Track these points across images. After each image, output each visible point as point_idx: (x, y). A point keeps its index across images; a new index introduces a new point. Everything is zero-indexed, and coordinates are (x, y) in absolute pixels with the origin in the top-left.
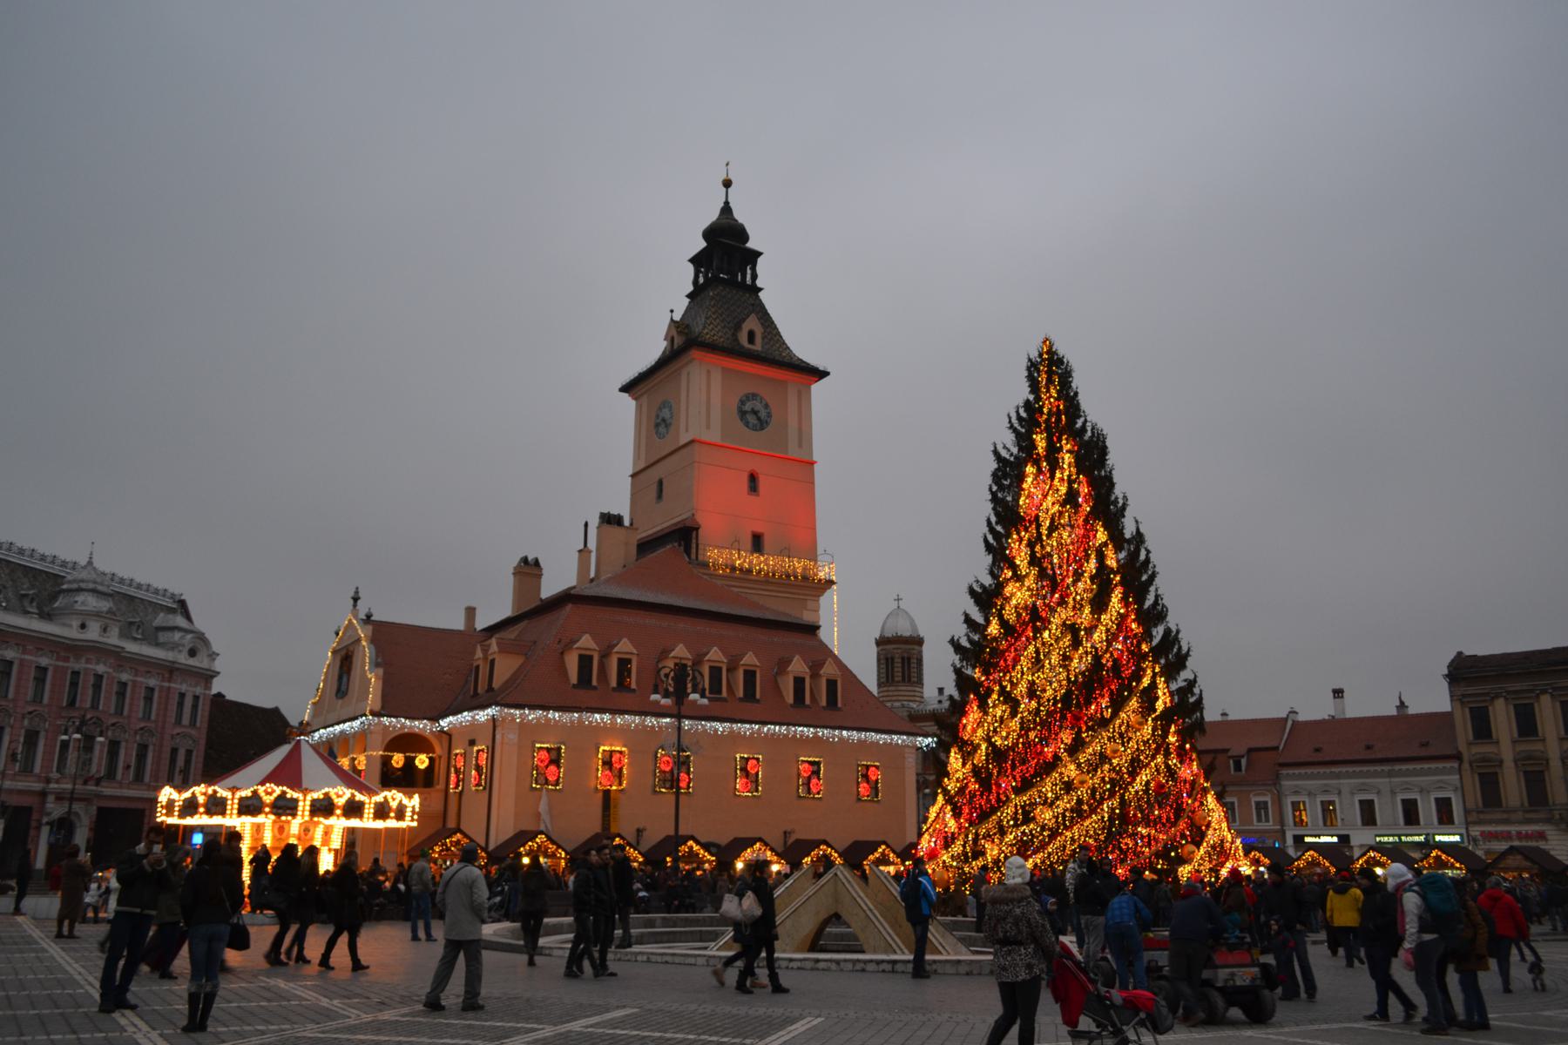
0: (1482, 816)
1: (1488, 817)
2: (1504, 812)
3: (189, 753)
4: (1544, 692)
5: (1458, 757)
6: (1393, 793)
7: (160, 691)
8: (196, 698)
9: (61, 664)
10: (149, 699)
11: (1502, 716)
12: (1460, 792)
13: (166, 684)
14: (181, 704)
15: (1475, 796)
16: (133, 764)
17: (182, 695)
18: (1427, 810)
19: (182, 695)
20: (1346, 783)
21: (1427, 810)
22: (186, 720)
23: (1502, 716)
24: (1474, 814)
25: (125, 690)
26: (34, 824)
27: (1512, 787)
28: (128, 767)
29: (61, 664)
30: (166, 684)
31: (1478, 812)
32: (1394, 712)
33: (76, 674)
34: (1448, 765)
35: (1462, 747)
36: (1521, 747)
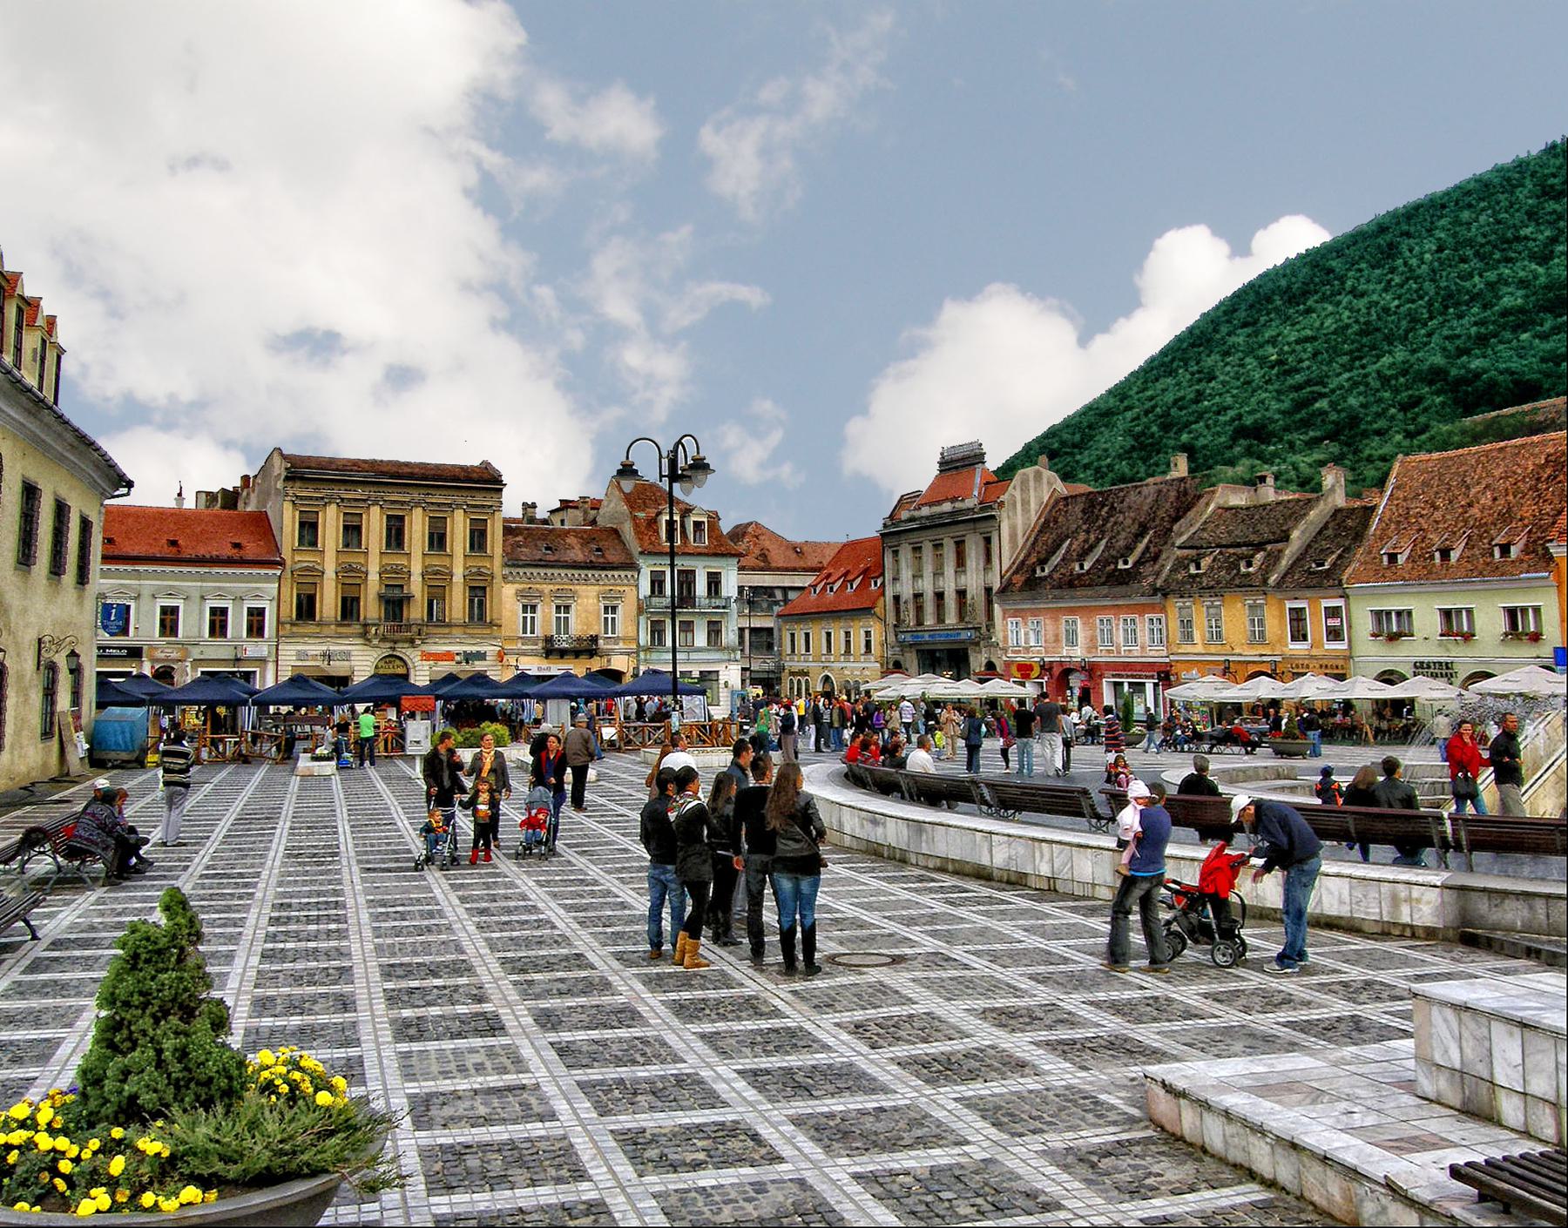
0: (295, 629)
1: (301, 630)
2: (318, 625)
4: (376, 503)
5: (282, 563)
6: (203, 598)
11: (331, 522)
12: (275, 604)
15: (290, 609)
18: (237, 623)
20: (149, 584)
21: (237, 623)
23: (331, 522)
24: (288, 626)
27: (329, 602)
31: (293, 625)
32: (173, 504)
34: (270, 572)
35: (286, 553)
36: (344, 558)
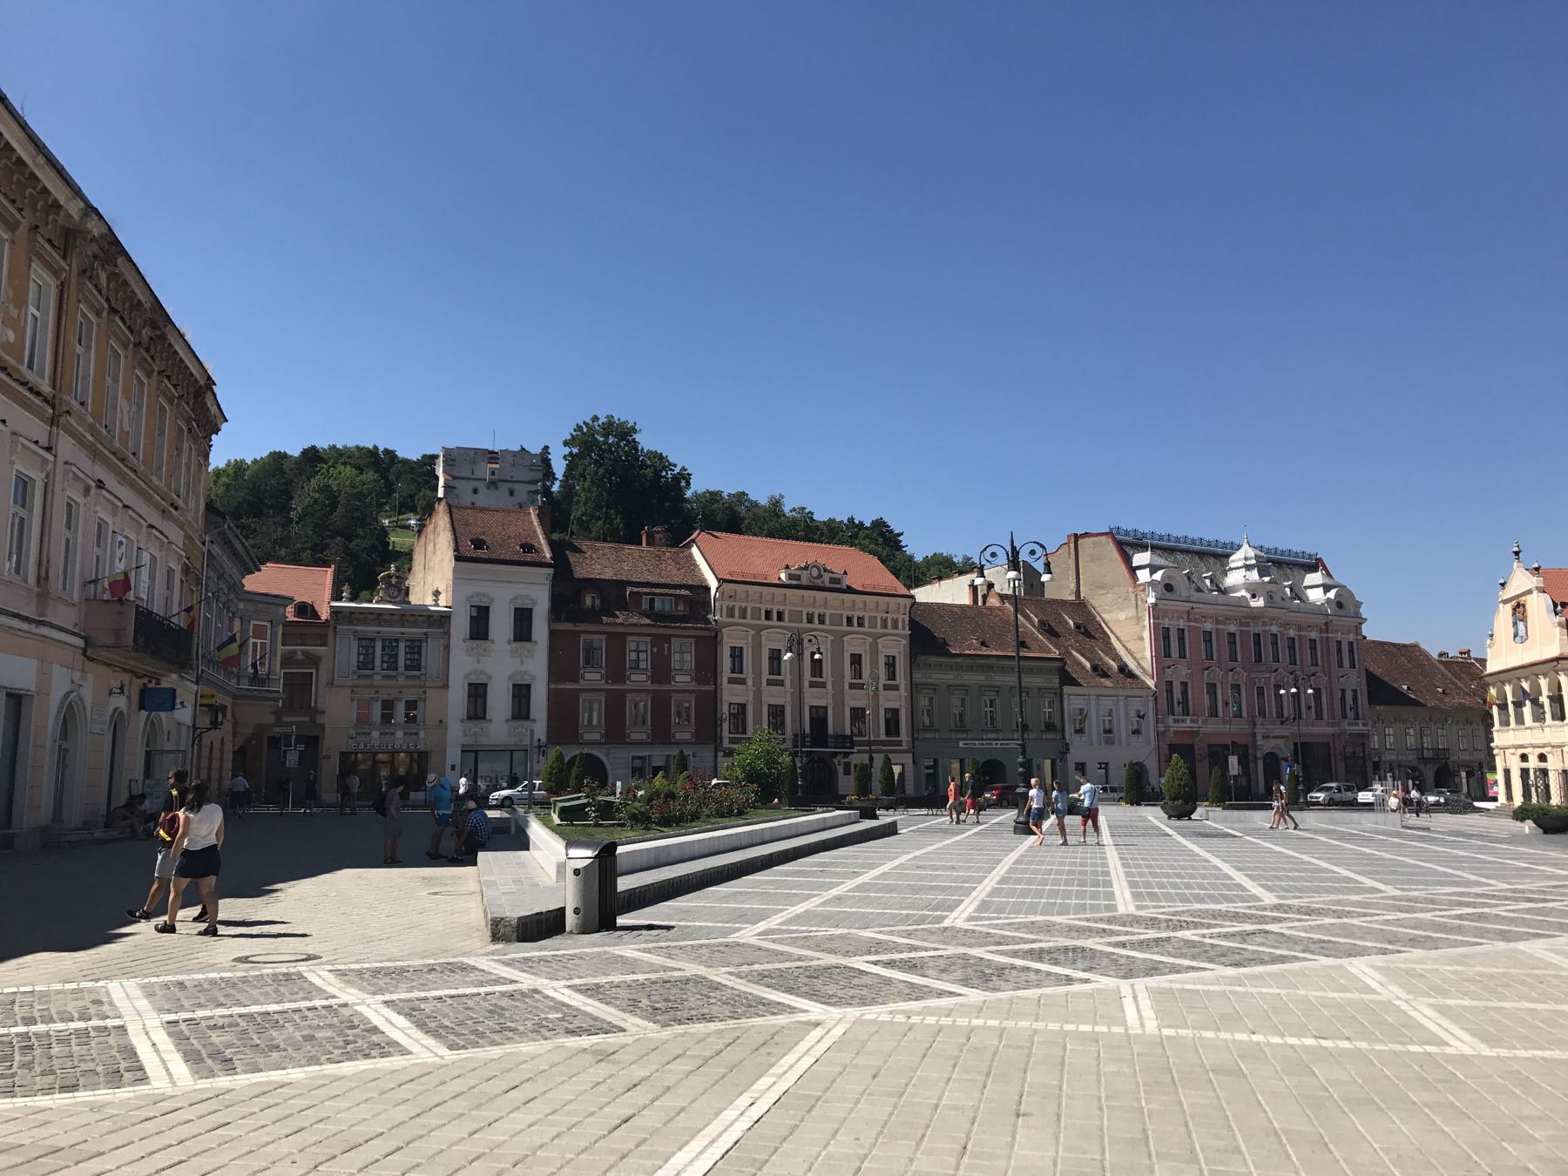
3: (1355, 691)
7: (1321, 642)
8: (1351, 644)
9: (1244, 628)
10: (1313, 648)
13: (1325, 635)
14: (1339, 650)
16: (1313, 704)
17: (1339, 643)
19: (1339, 643)
22: (1346, 662)
25: (1294, 642)
26: (1251, 758)
28: (1310, 708)
29: (1244, 628)
30: (1325, 635)
33: (1257, 636)
